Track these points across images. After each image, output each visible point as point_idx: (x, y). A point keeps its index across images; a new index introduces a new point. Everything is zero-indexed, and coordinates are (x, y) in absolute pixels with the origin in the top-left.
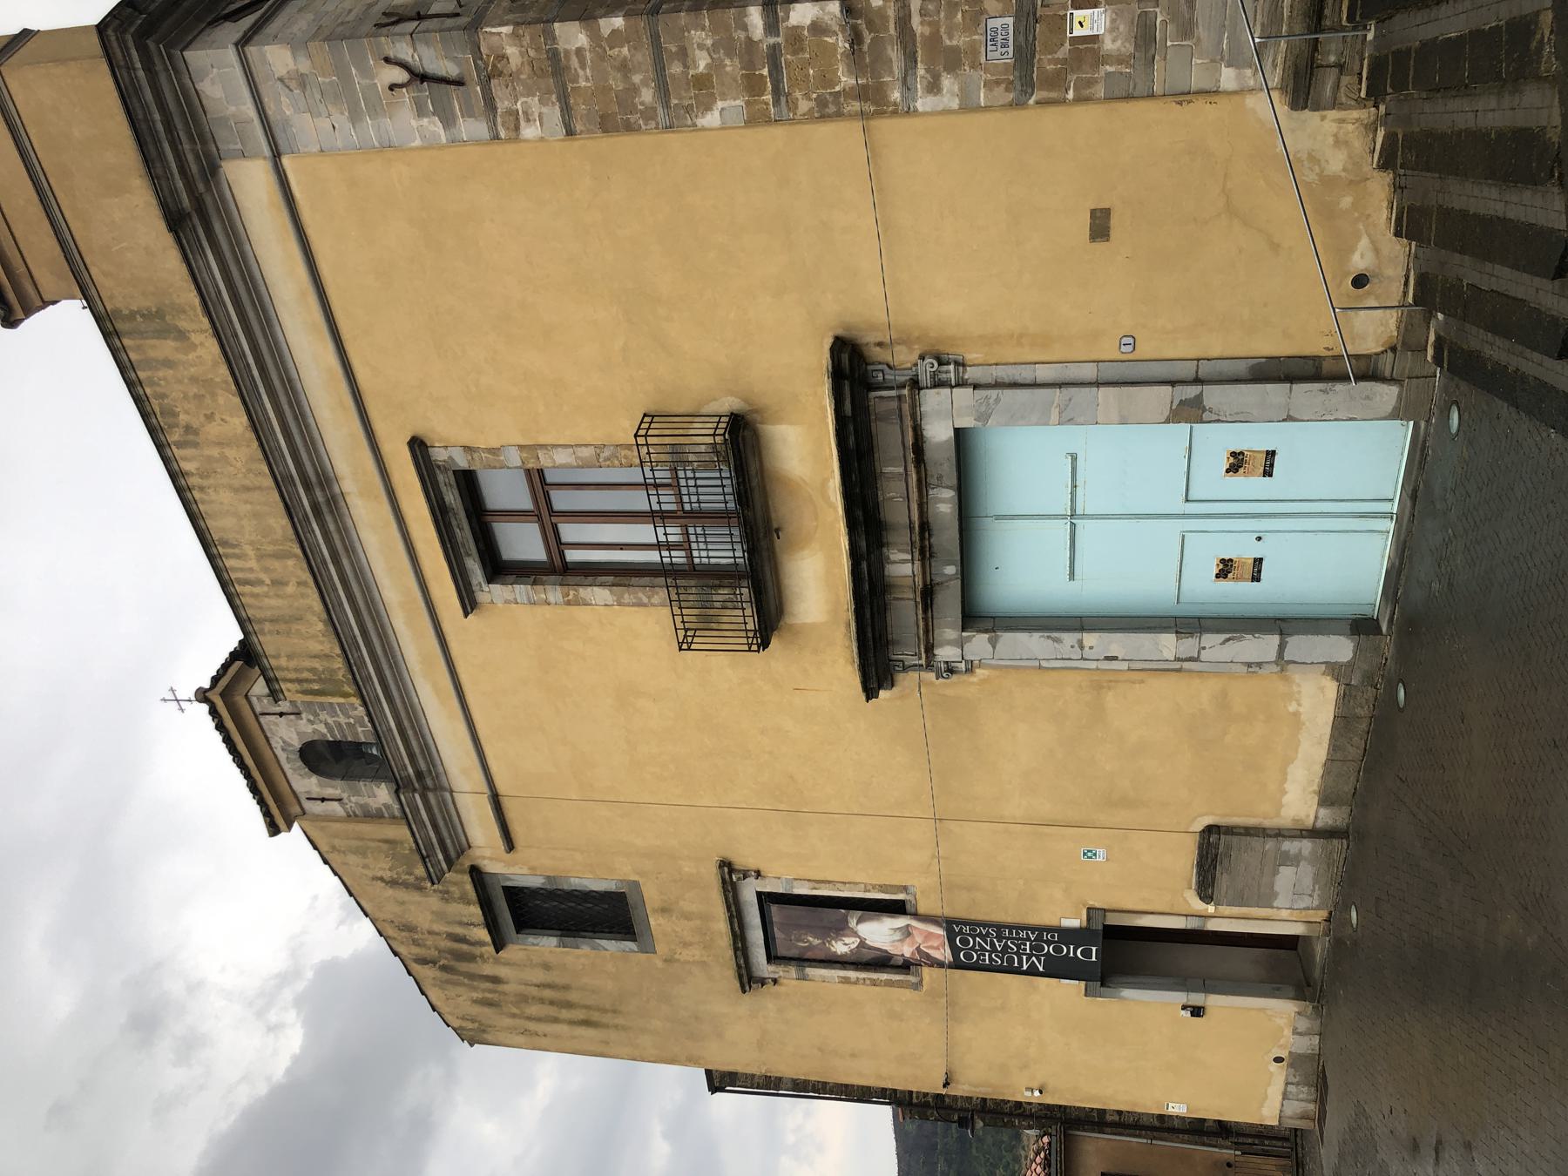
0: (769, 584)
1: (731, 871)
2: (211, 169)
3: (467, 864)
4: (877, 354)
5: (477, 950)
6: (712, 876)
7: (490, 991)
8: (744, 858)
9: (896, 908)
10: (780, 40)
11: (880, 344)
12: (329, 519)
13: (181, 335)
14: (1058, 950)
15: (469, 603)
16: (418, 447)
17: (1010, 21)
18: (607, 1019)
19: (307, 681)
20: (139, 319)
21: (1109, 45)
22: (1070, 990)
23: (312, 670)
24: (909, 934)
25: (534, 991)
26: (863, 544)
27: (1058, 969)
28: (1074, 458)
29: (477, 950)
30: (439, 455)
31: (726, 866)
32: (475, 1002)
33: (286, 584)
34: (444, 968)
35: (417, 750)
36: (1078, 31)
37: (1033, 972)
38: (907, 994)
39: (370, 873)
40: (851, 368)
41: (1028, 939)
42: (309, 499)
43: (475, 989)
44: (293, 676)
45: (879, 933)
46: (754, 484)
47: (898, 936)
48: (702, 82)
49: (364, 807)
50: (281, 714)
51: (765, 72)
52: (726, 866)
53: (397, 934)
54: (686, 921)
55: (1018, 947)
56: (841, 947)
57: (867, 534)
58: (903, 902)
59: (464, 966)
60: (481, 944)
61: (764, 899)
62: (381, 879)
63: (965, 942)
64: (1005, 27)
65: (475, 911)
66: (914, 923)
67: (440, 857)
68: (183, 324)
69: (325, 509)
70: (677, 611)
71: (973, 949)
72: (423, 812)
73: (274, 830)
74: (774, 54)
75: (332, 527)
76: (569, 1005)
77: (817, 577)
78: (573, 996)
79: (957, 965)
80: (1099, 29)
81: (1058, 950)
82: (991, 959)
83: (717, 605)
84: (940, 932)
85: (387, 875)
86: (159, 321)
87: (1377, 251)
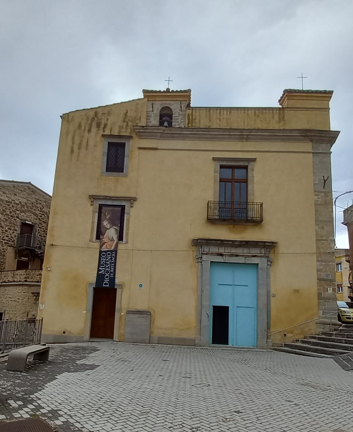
0: (225, 223)
1: (134, 200)
2: (311, 141)
3: (134, 135)
4: (272, 251)
5: (101, 129)
6: (131, 194)
7: (85, 128)
8: (136, 204)
9: (120, 238)
10: (329, 241)
11: (274, 251)
12: (239, 137)
13: (279, 122)
14: (107, 277)
15: (214, 159)
16: (254, 160)
17: (331, 278)
18: (75, 156)
19: (192, 117)
20: (283, 116)
21: (326, 293)
22: (93, 278)
23: (195, 119)
24: (111, 241)
25: (85, 141)
26: (236, 243)
27: (100, 277)
28: (247, 286)
29: (101, 129)
30: (252, 163)
31: (135, 199)
32: (80, 123)
33: (220, 121)
34: (93, 119)
35: (174, 135)
36: (329, 288)
37: (99, 270)
38: (88, 237)
39: (129, 111)
40: (269, 247)
41: (111, 270)
42: (245, 135)
43: (86, 124)
44: (194, 113)
45: (111, 233)
46: (248, 224)
47: (111, 238)
48: (323, 228)
49: (150, 116)
50: (181, 107)
51: (324, 238)
52: (135, 199)
53: (108, 110)
54: (114, 187)
55: (108, 267)
56: (105, 223)
57: (238, 244)
58: (122, 240)
59: (94, 124)
60: (104, 131)
61: (123, 207)
62: (127, 112)
63: (109, 254)
64: (330, 277)
65: (116, 133)
66: (115, 242)
67: (141, 131)
68: (281, 123)
69: (241, 137)
70: (231, 203)
71: (106, 256)
72: (156, 131)
73: (145, 91)
74: (327, 240)
75: (237, 137)
76: (79, 148)
77: (222, 233)
78: (83, 150)
79: (101, 252)
80: (329, 292)
81: (107, 277)
82: (103, 260)
83: (215, 211)
84: (112, 248)
85: (129, 114)
86: (282, 119)
87: (290, 338)
